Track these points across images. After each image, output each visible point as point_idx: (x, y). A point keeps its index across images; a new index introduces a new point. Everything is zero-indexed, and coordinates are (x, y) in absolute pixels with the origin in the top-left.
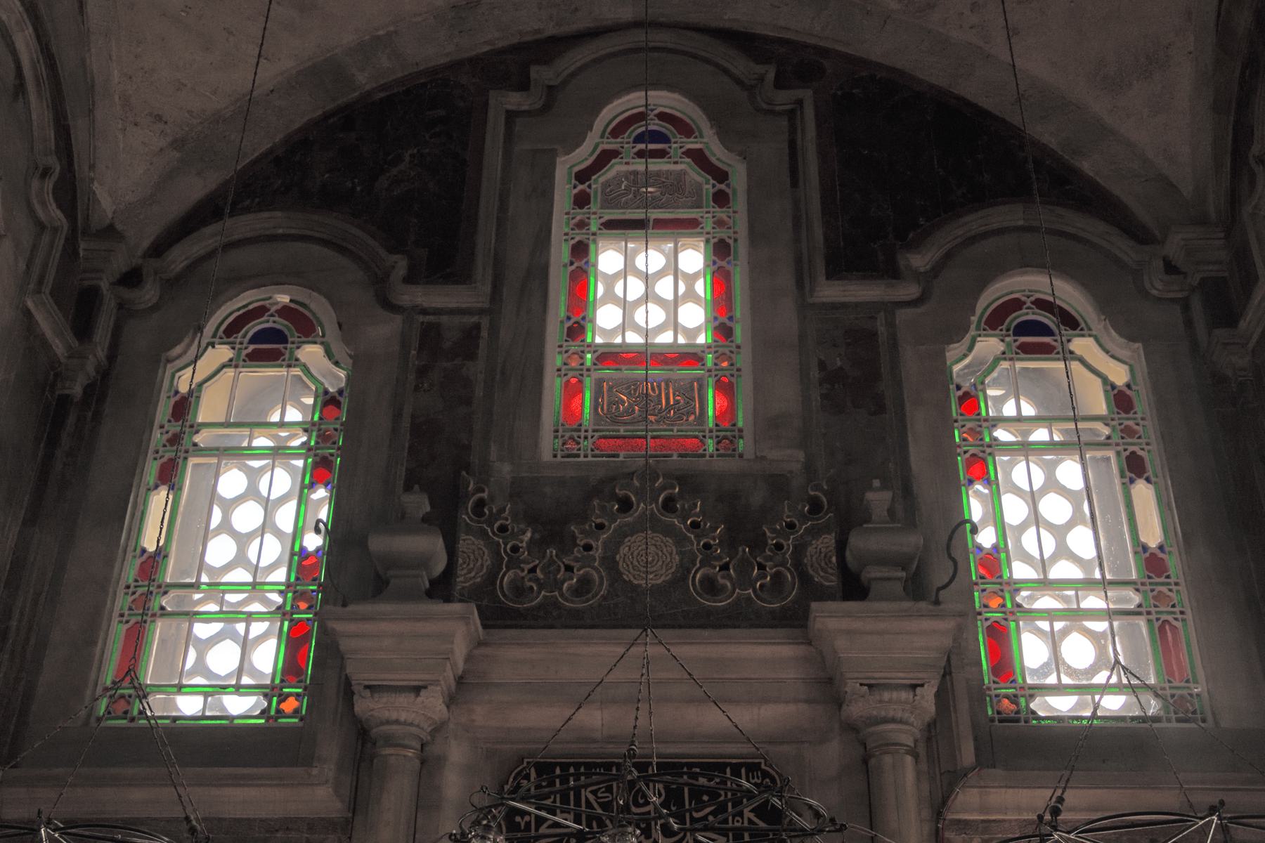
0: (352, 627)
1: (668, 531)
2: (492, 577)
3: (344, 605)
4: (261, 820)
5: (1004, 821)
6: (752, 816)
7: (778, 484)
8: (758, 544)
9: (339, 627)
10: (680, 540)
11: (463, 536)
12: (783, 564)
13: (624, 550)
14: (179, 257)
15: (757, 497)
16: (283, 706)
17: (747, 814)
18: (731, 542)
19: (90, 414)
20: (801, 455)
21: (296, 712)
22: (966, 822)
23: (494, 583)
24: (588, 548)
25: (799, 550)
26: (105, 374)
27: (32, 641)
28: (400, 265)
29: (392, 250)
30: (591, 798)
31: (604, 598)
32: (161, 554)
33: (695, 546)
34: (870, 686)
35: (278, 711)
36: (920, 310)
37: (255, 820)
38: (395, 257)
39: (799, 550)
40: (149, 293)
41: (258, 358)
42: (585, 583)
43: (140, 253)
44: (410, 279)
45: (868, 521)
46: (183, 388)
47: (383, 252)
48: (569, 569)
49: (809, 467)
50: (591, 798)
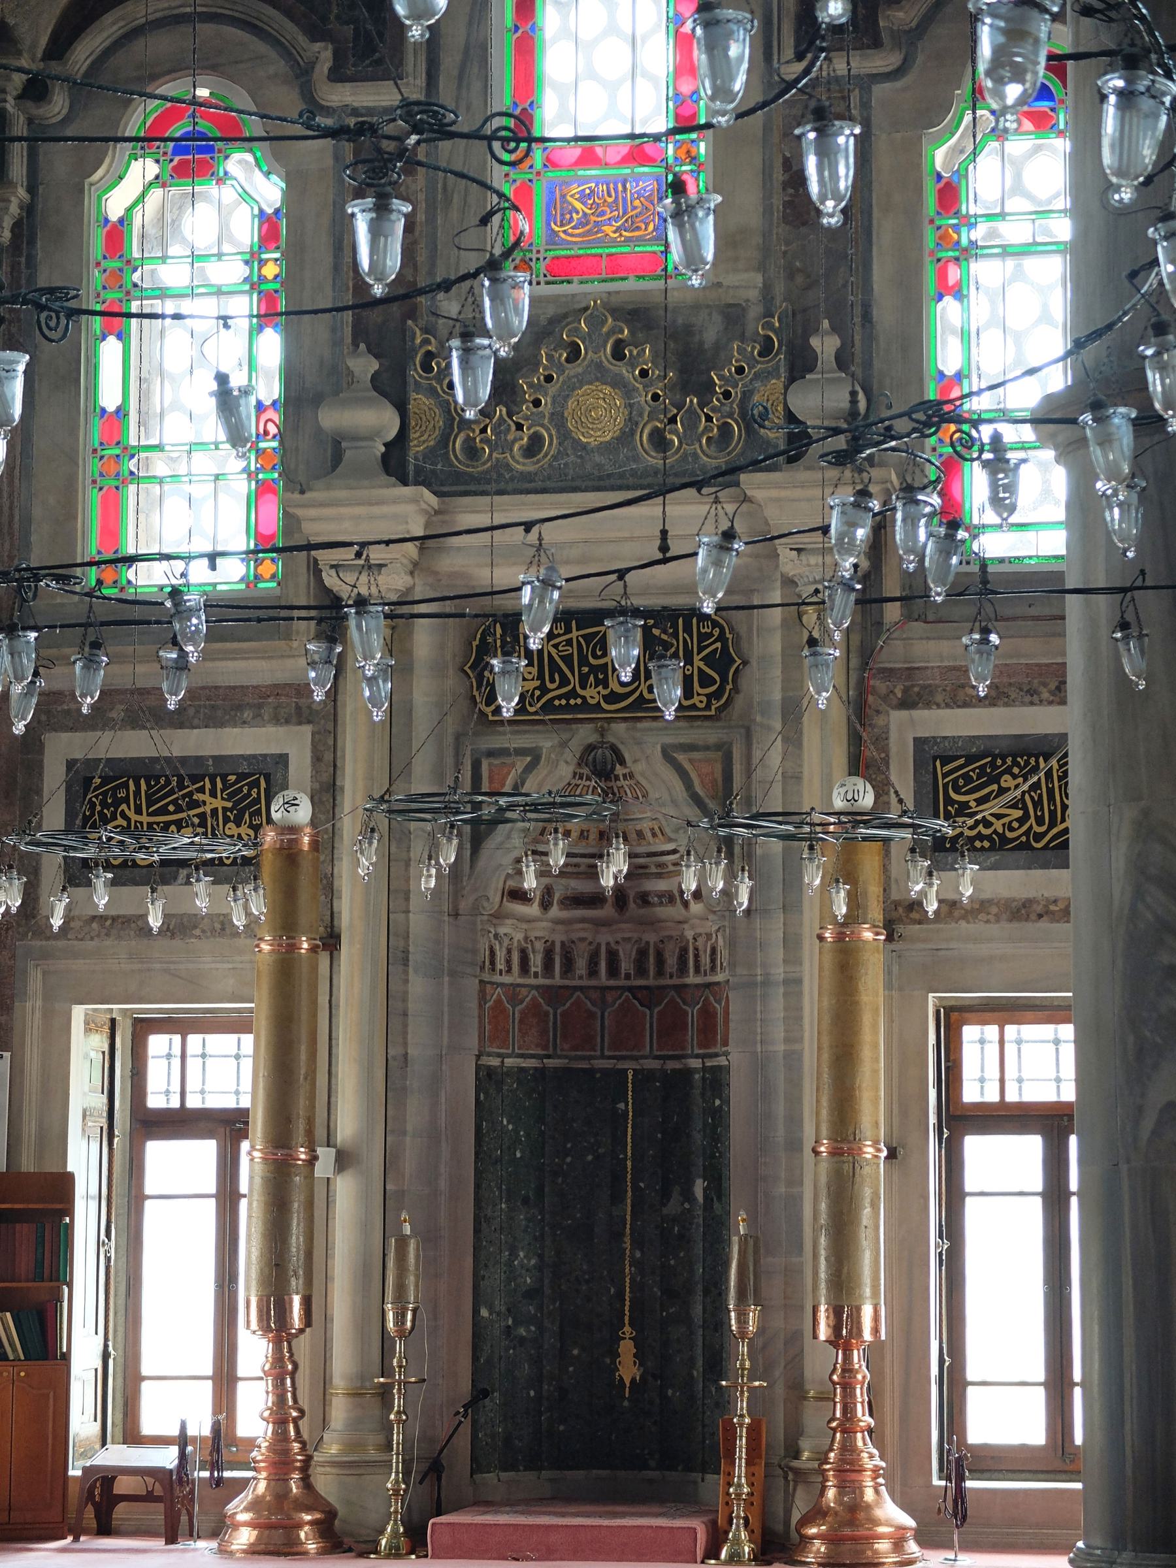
0: (312, 512)
1: (618, 383)
2: (445, 440)
3: (302, 492)
4: (253, 687)
5: (927, 668)
6: (702, 665)
7: (733, 315)
8: (705, 390)
9: (299, 512)
10: (628, 392)
11: (414, 395)
12: (731, 416)
13: (571, 404)
14: (83, 54)
15: (711, 333)
16: (260, 569)
17: (698, 662)
18: (685, 386)
19: (23, 260)
20: (759, 279)
21: (273, 576)
22: (891, 670)
23: (446, 446)
24: (537, 403)
25: (747, 395)
26: (29, 209)
27: (17, 518)
28: (324, 54)
29: (314, 40)
30: (554, 652)
31: (555, 458)
32: (121, 412)
33: (643, 399)
34: (799, 550)
35: (256, 577)
36: (898, 84)
37: (247, 687)
38: (318, 46)
39: (747, 395)
40: (58, 104)
41: (184, 171)
42: (536, 443)
43: (39, 55)
44: (337, 75)
45: (811, 370)
46: (114, 217)
47: (302, 40)
48: (519, 427)
49: (767, 289)
50: (554, 652)
